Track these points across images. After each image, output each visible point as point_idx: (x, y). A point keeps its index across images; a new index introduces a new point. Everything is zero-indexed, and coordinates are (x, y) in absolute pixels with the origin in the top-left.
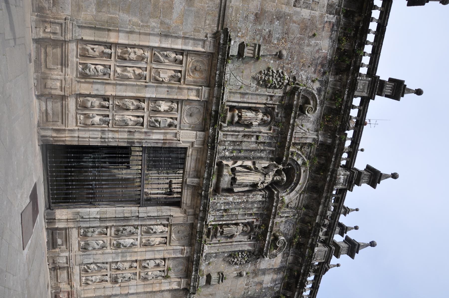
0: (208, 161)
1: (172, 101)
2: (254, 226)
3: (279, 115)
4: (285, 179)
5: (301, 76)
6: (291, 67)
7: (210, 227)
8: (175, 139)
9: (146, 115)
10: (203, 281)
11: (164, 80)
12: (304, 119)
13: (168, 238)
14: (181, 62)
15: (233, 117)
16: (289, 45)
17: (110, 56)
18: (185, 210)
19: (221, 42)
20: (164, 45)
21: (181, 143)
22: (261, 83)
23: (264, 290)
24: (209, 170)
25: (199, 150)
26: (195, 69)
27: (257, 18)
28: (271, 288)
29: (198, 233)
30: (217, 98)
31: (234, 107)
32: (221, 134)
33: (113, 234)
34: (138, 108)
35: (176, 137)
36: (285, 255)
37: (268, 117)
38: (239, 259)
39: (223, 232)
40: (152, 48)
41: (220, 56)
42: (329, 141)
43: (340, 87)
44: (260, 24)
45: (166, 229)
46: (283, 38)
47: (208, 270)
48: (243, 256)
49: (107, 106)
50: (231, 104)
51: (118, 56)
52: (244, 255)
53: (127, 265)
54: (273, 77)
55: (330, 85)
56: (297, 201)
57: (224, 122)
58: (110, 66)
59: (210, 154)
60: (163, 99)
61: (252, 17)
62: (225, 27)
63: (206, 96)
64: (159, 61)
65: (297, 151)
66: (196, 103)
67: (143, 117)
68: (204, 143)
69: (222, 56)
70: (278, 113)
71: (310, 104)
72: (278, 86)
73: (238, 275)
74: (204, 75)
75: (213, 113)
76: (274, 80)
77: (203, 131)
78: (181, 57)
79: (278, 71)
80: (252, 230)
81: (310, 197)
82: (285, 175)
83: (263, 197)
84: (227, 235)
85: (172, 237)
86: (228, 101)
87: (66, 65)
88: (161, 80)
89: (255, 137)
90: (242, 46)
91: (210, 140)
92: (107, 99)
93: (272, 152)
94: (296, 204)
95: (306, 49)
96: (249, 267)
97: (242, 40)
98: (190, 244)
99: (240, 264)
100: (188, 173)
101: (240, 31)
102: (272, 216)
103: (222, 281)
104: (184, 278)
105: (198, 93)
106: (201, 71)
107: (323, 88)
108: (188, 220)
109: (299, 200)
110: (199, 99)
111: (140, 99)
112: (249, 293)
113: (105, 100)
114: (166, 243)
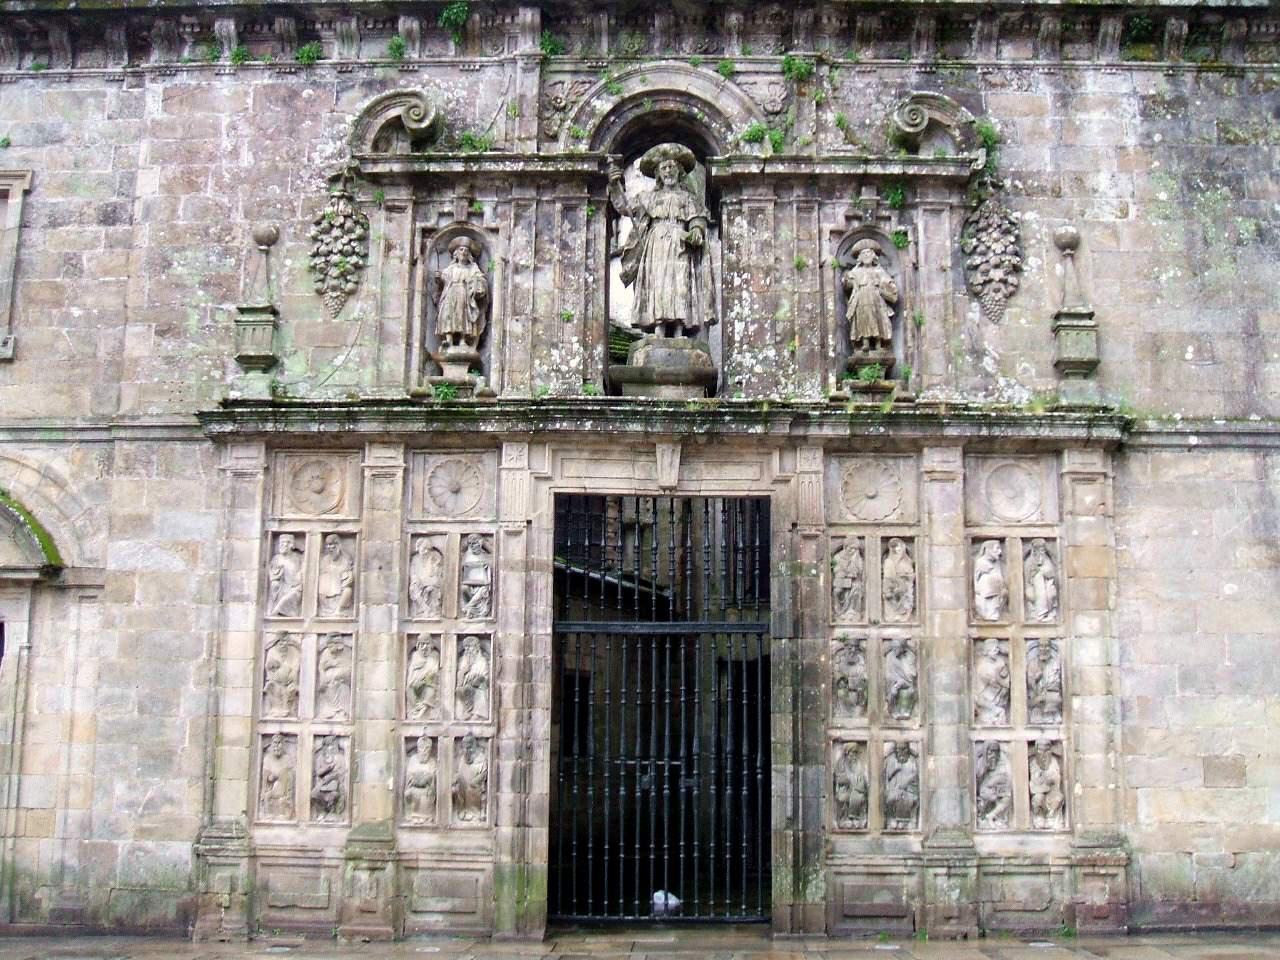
0: (588, 425)
2: (856, 224)
3: (446, 210)
4: (666, 146)
5: (332, 156)
6: (302, 196)
7: (846, 391)
8: (524, 534)
10: (1081, 392)
11: (346, 583)
12: (464, 120)
13: (889, 532)
14: (300, 536)
15: (456, 360)
16: (238, 217)
18: (776, 482)
19: (229, 428)
20: (251, 586)
21: (539, 517)
22: (350, 286)
23: (1157, 138)
24: (615, 420)
25: (561, 455)
26: (319, 492)
27: (169, 330)
28: (1150, 107)
29: (858, 431)
30: (388, 421)
31: (427, 358)
32: (508, 394)
35: (520, 533)
36: (995, 78)
37: (457, 247)
38: (994, 260)
41: (270, 427)
43: (349, 22)
44: (185, 317)
46: (219, 241)
47: (1040, 375)
48: (982, 248)
49: (429, 743)
50: (414, 374)
51: (289, 715)
52: (975, 248)
54: (330, 252)
55: (350, 54)
56: (762, 79)
57: (472, 385)
58: (316, 736)
59: (562, 420)
61: (169, 345)
62: (194, 421)
63: (391, 453)
65: (568, 123)
66: (418, 480)
67: (460, 637)
68: (536, 439)
69: (267, 421)
70: (442, 215)
71: (399, 118)
72: (359, 231)
73: (1072, 256)
74: (334, 462)
76: (340, 247)
77: (499, 448)
78: (283, 539)
79: (315, 239)
80: (871, 232)
81: (745, 34)
82: (652, 151)
83: (740, 212)
84: (887, 321)
85: (887, 520)
87: (317, 855)
88: (348, 590)
89: (518, 279)
90: (247, 363)
91: (521, 426)
92: (411, 745)
93: (568, 209)
94: (772, 83)
97: (232, 364)
98: (916, 448)
99: (1016, 254)
100: (636, 485)
101: (208, 373)
102: (804, 169)
103: (1090, 316)
104: (1060, 465)
105: (382, 475)
106: (324, 479)
107: (363, 75)
108: (814, 468)
109: (757, 73)
110: (400, 473)
112: (1163, 196)
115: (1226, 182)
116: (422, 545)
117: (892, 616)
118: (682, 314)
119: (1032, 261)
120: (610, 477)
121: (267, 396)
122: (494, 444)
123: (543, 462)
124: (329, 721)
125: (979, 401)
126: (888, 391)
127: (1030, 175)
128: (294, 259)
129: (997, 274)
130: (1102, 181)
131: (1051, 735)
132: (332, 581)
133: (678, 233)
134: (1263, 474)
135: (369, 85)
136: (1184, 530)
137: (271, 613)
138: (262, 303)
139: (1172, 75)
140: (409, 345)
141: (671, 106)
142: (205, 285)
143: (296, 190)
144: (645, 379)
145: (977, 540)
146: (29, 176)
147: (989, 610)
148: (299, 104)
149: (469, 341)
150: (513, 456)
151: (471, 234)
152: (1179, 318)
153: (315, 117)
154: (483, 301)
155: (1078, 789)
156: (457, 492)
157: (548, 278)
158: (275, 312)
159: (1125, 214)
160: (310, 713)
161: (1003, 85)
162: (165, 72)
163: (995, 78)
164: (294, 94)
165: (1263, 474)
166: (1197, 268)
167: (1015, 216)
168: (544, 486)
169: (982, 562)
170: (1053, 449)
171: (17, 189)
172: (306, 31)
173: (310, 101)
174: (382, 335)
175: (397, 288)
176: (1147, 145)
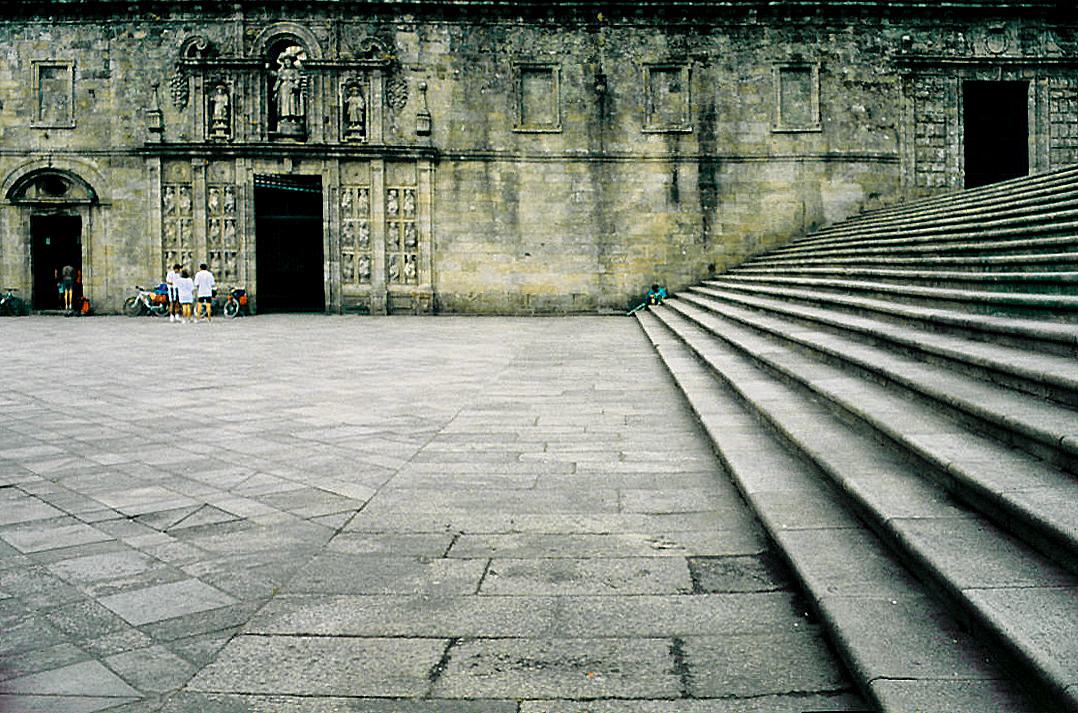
1: (208, 194)
9: (225, 218)
14: (173, 188)
17: (174, 253)
33: (352, 248)
34: (218, 223)
39: (356, 123)
40: (163, 217)
50: (206, 135)
53: (392, 233)
60: (207, 203)
64: (173, 210)
68: (246, 157)
72: (186, 83)
80: (356, 85)
86: (204, 137)
90: (153, 130)
96: (413, 79)
111: (209, 224)
113: (212, 256)
116: (212, 190)
117: (361, 215)
118: (293, 113)
119: (411, 94)
120: (273, 169)
121: (159, 142)
122: (232, 159)
123: (249, 163)
124: (187, 248)
126: (360, 140)
128: (165, 93)
129: (398, 100)
131: (413, 253)
132: (185, 202)
133: (291, 85)
135: (186, 30)
137: (166, 212)
138: (156, 109)
142: (136, 102)
144: (282, 136)
145: (389, 190)
146: (70, 66)
147: (393, 213)
149: (224, 122)
150: (239, 162)
151: (224, 84)
155: (420, 271)
156: (223, 173)
158: (159, 111)
160: (180, 245)
165: (487, 168)
167: (406, 78)
169: (390, 197)
170: (414, 161)
171: (70, 66)
172: (164, 11)
175: (200, 103)
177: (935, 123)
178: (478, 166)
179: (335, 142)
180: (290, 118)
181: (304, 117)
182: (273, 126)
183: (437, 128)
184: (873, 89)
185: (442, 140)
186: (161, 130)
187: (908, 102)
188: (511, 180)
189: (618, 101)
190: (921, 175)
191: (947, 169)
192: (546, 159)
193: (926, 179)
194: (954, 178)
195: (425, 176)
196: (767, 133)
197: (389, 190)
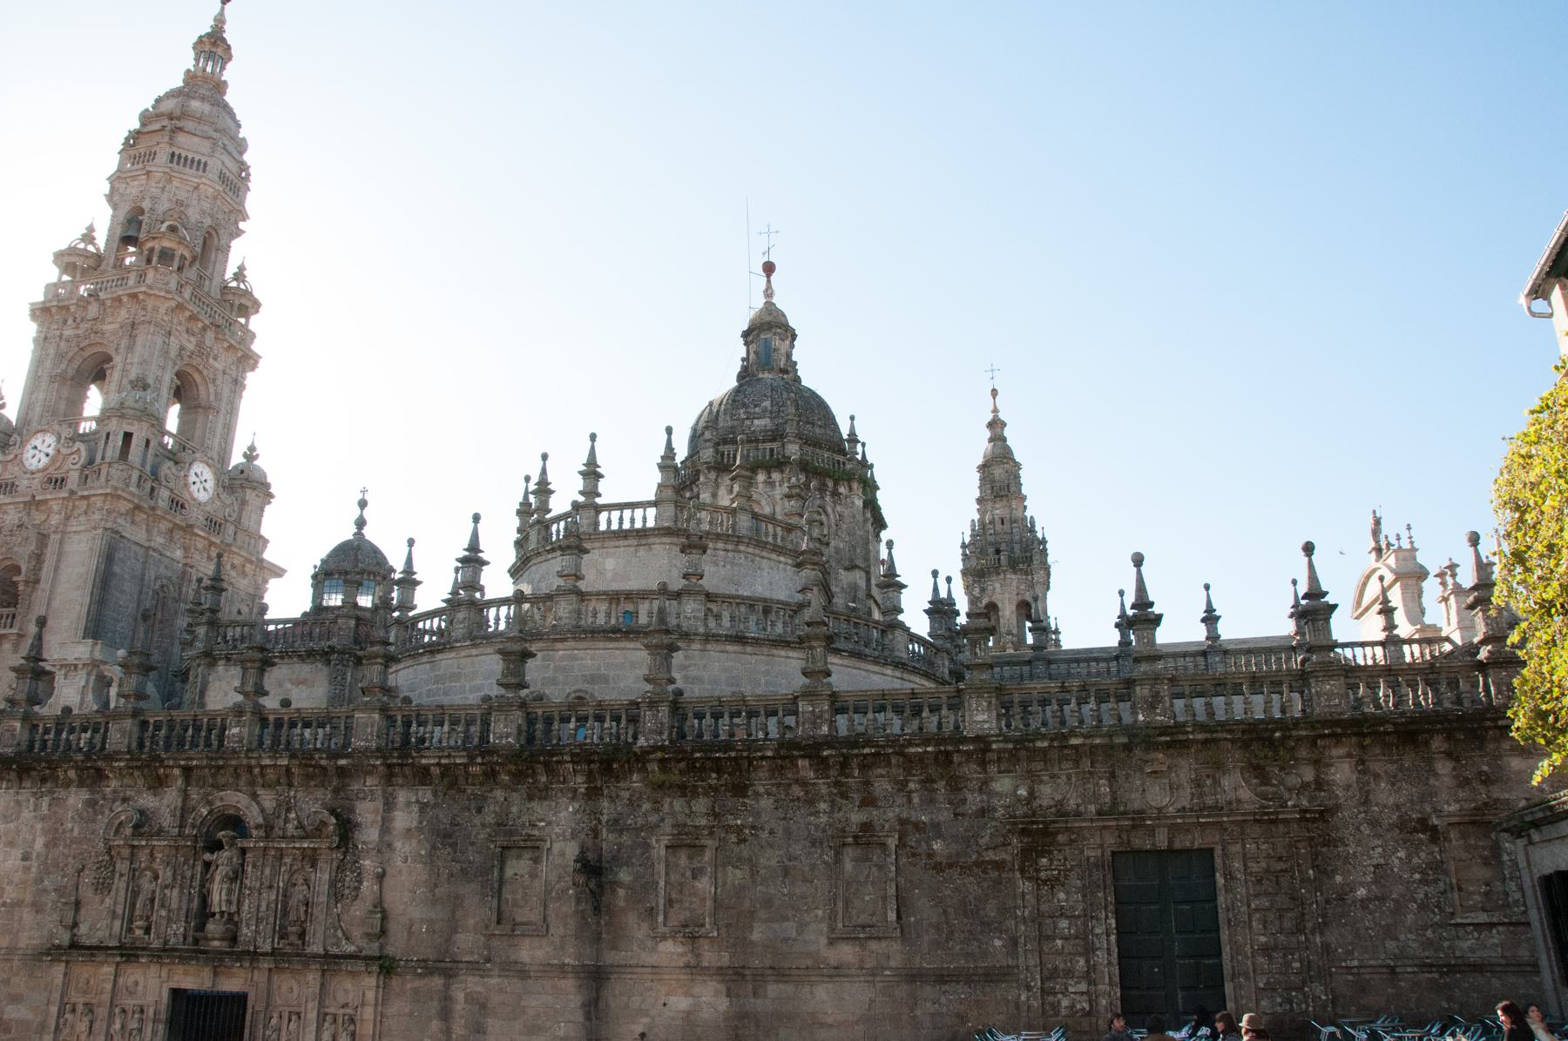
4: (223, 833)
15: (138, 927)
23: (425, 823)
28: (423, 807)
42: (177, 772)
44: (46, 904)
45: (276, 1015)
75: (124, 959)
95: (76, 831)
96: (367, 863)
112: (423, 852)
114: (298, 1014)
115: (451, 846)
118: (224, 909)
119: (365, 884)
125: (334, 950)
127: (371, 843)
128: (87, 879)
130: (398, 844)
134: (447, 987)
136: (411, 1014)
139: (435, 794)
140: (123, 919)
141: (231, 812)
142: (55, 890)
143: (93, 847)
145: (326, 1014)
148: (98, 807)
152: (417, 912)
153: (103, 813)
154: (152, 900)
157: (176, 892)
159: (406, 861)
161: (364, 799)
162: (51, 792)
163: (361, 795)
164: (96, 803)
166: (432, 891)
168: (165, 985)
173: (102, 806)
174: (114, 915)
176: (420, 830)
177: (1067, 917)
178: (437, 982)
179: (268, 948)
180: (222, 913)
181: (238, 912)
182: (201, 927)
183: (393, 927)
184: (976, 870)
185: (397, 945)
186: (75, 925)
187: (1025, 886)
188: (481, 1006)
189: (621, 892)
190: (1051, 998)
191: (1092, 988)
192: (523, 973)
193: (1059, 1002)
194: (1104, 1002)
195: (370, 995)
196: (823, 941)
197: (326, 1014)
